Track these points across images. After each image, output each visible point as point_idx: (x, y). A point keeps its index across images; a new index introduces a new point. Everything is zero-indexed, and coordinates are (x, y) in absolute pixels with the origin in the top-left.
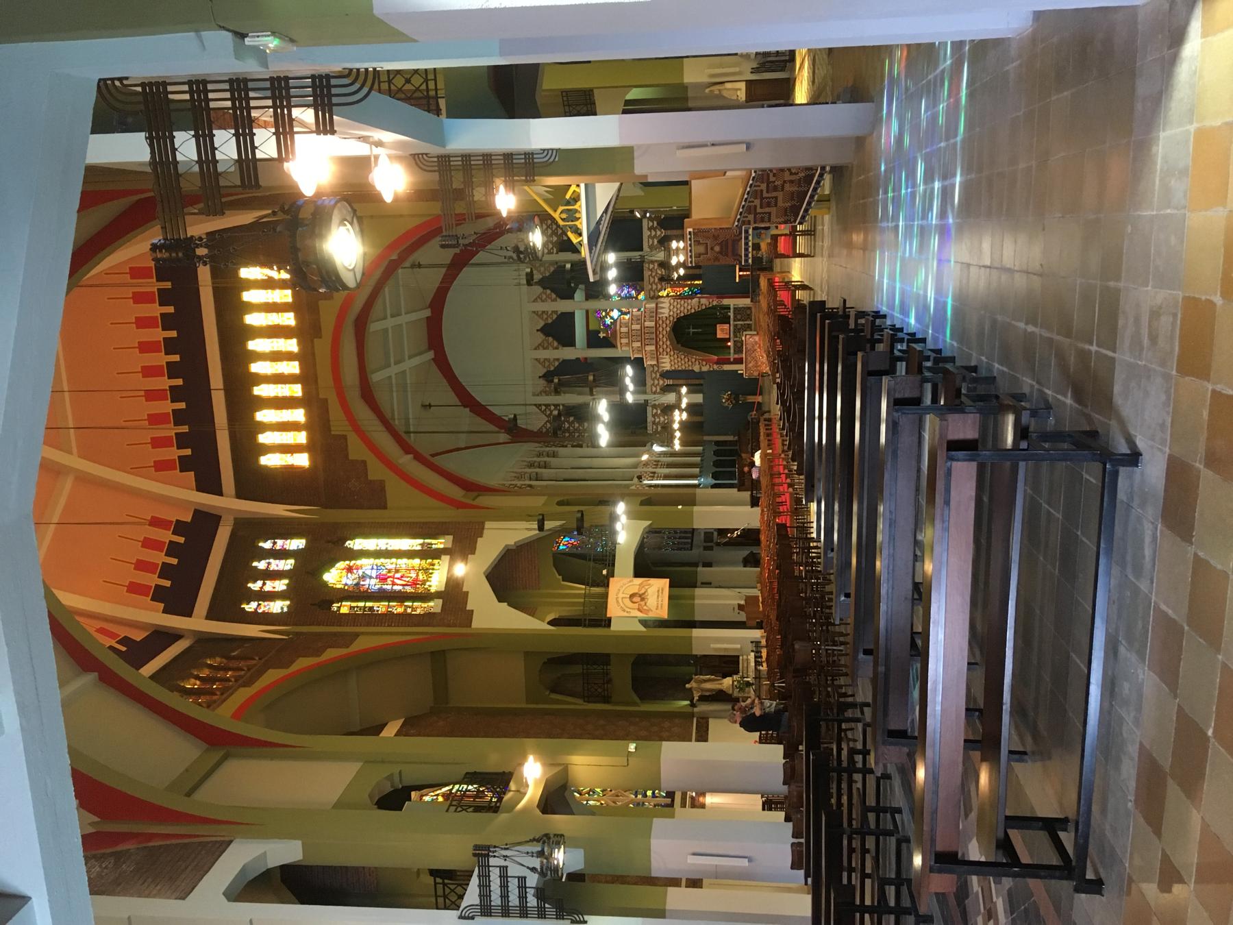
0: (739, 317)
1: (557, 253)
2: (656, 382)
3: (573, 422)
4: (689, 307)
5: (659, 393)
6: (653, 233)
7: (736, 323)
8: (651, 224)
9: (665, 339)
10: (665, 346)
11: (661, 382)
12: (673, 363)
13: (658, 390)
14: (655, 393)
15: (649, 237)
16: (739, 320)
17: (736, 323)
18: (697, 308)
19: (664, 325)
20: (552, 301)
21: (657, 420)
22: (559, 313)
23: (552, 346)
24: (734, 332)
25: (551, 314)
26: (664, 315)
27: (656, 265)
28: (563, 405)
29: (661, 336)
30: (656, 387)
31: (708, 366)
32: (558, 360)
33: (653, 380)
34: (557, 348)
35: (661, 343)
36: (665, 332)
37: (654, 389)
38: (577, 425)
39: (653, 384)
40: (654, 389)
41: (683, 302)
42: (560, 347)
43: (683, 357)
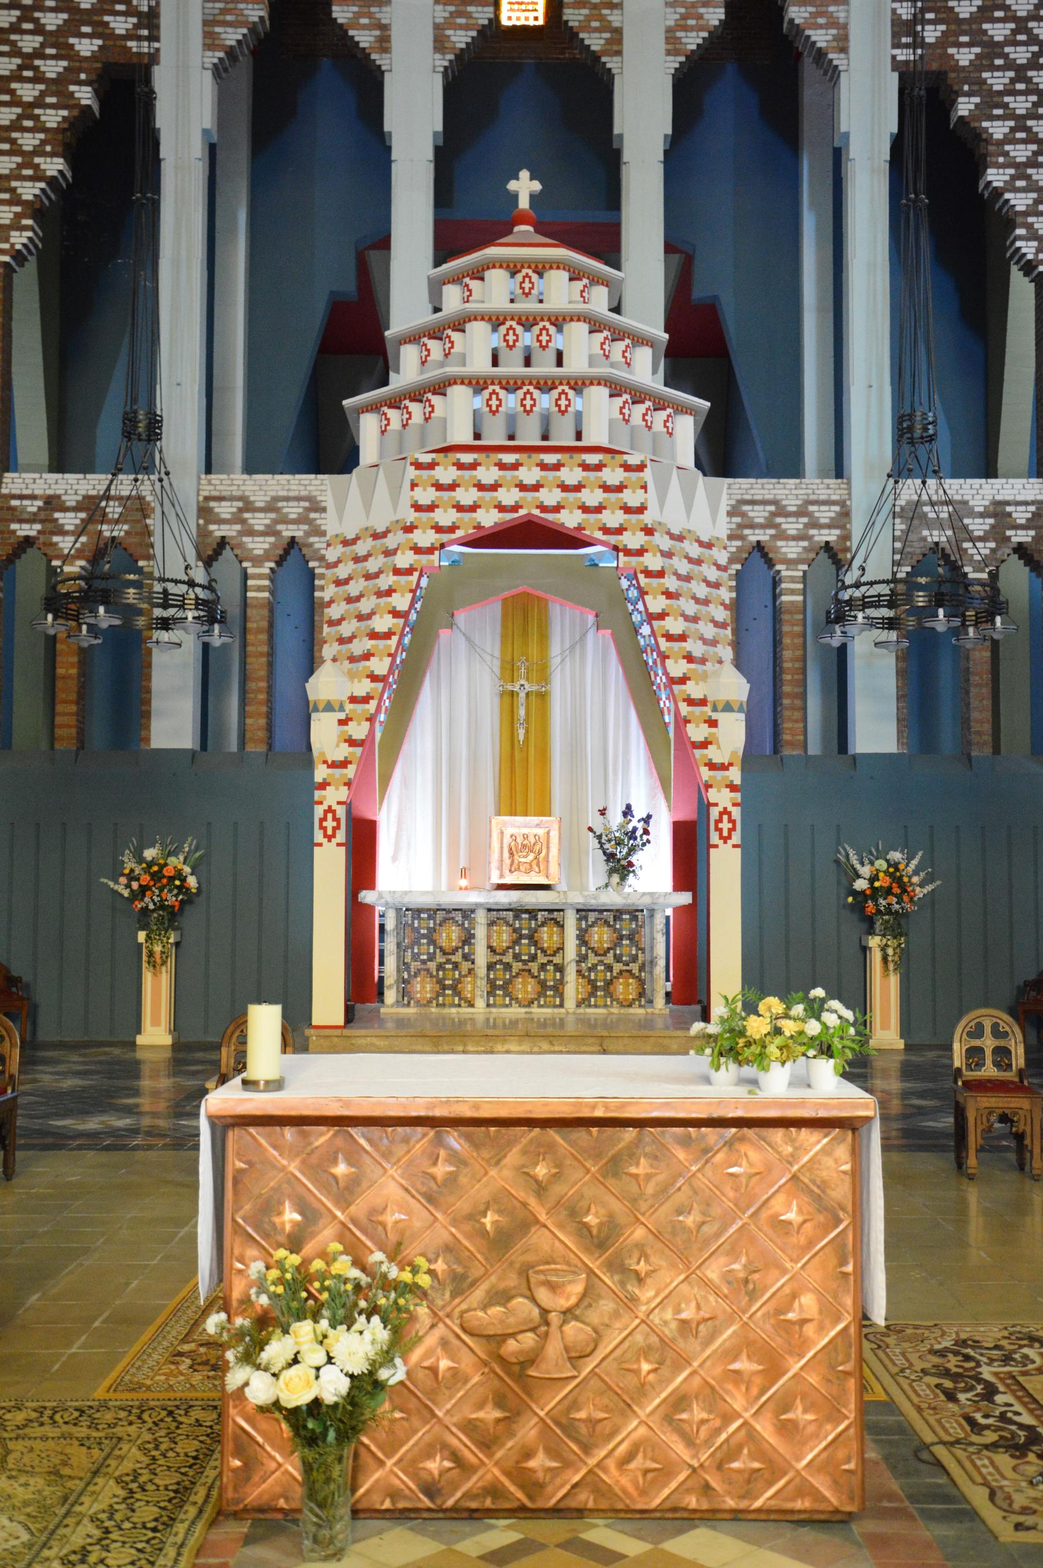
0: (600, 936)
1: (896, 65)
2: (259, 521)
3: (66, 101)
4: (697, 649)
5: (203, 533)
6: (978, 526)
7: (571, 921)
8: (1021, 515)
9: (508, 496)
10: (467, 496)
11: (259, 545)
12: (361, 548)
13: (218, 531)
14: (204, 512)
15: (960, 509)
16: (582, 939)
17: (571, 921)
18: (692, 689)
19: (592, 497)
20: (670, 34)
21: (69, 520)
22: (611, 63)
23: (449, 23)
24: (518, 912)
25: (606, 27)
26: (651, 498)
27: (831, 536)
28: (154, 58)
29: (529, 475)
30: (237, 519)
31: (343, 751)
32: (384, 43)
33: (269, 508)
34: (440, 44)
35: (488, 474)
36: (550, 496)
37: (225, 509)
38: (52, 118)
39: (248, 506)
40: (225, 509)
41: (721, 614)
42: (442, 61)
43: (401, 601)
